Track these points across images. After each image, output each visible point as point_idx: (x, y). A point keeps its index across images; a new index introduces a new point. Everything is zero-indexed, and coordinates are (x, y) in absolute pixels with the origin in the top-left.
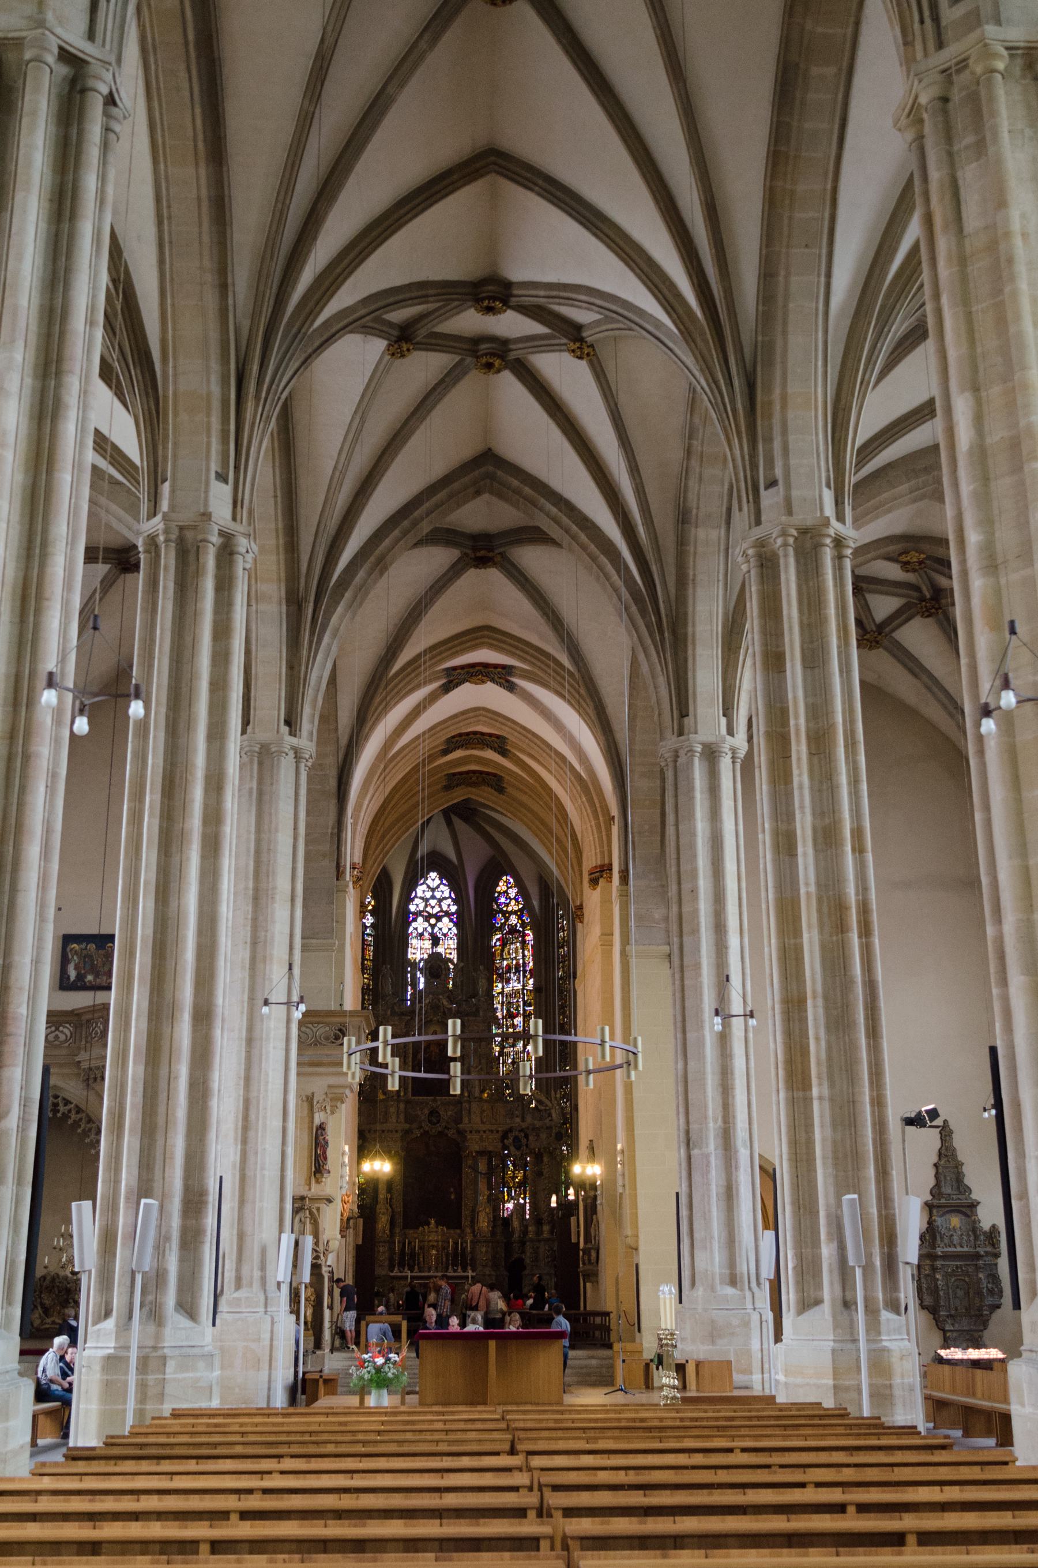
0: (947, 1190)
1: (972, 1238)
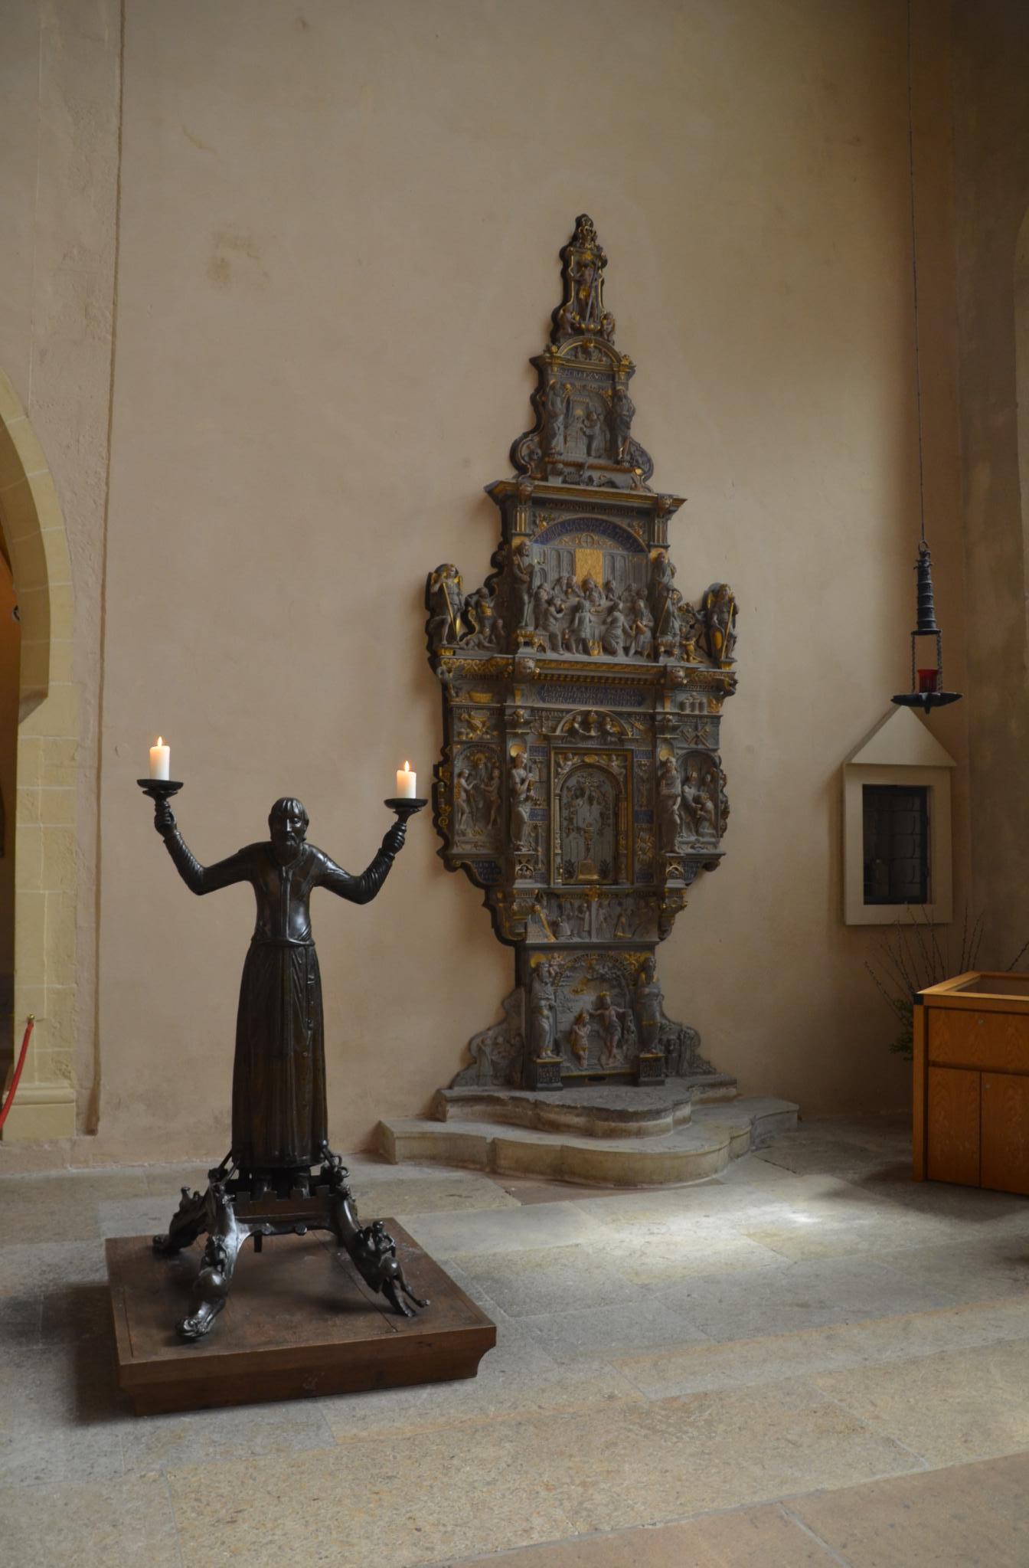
0: (570, 448)
1: (645, 622)
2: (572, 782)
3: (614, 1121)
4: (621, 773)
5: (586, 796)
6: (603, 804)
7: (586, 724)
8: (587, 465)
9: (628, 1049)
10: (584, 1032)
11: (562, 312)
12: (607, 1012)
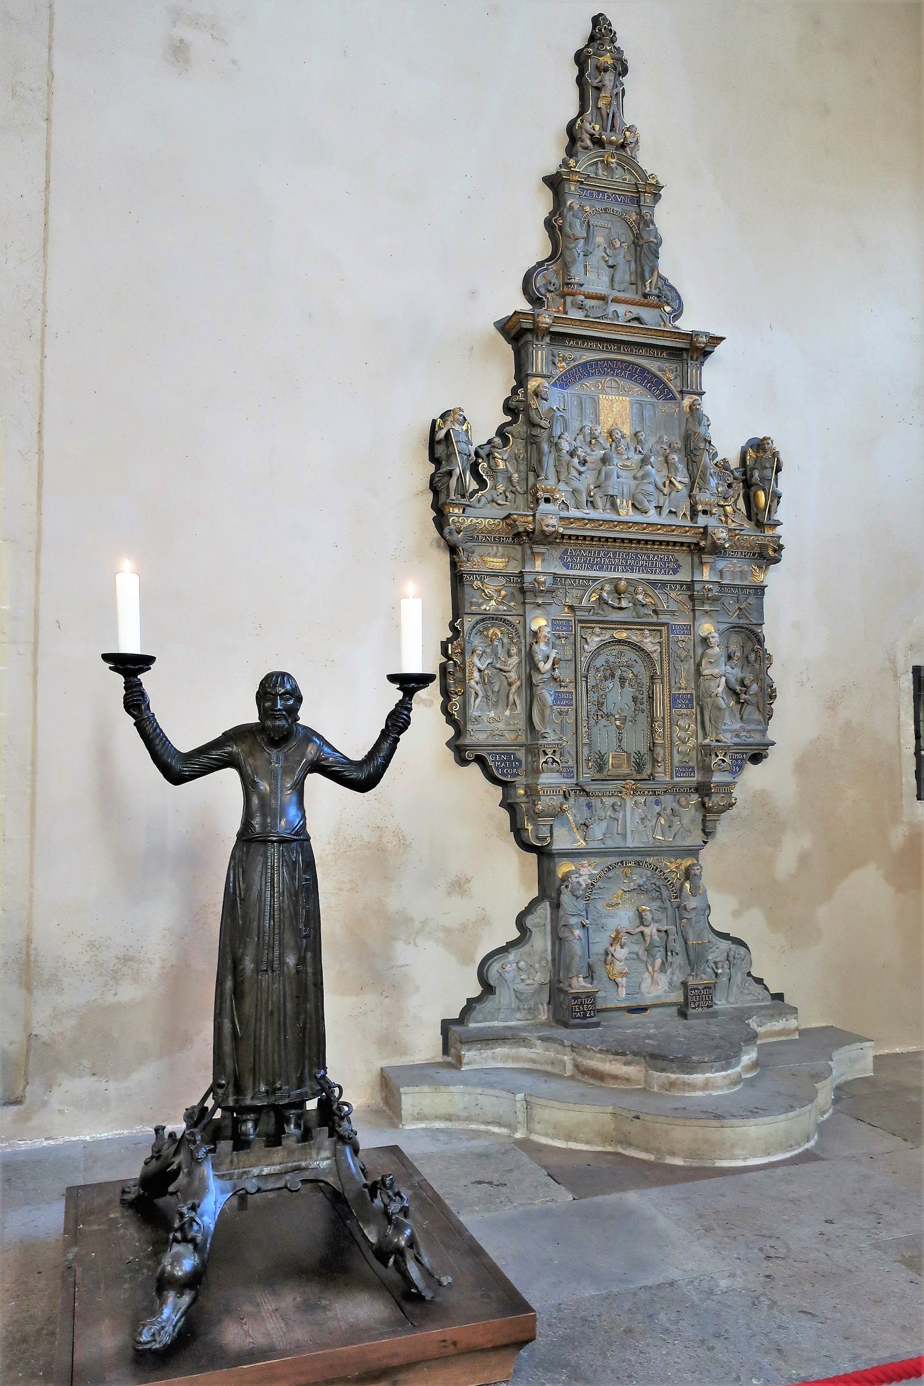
2: (600, 661)
3: (673, 1072)
4: (655, 651)
5: (617, 678)
6: (636, 687)
7: (618, 592)
8: (611, 298)
9: (673, 974)
10: (620, 953)
11: (579, 121)
12: (647, 931)
